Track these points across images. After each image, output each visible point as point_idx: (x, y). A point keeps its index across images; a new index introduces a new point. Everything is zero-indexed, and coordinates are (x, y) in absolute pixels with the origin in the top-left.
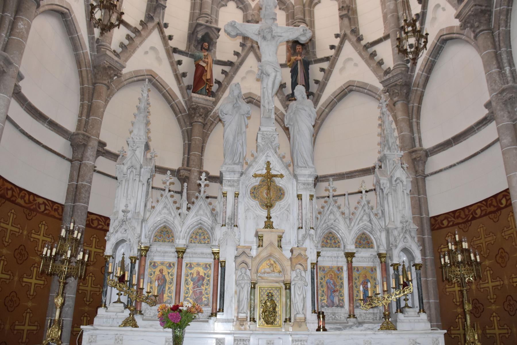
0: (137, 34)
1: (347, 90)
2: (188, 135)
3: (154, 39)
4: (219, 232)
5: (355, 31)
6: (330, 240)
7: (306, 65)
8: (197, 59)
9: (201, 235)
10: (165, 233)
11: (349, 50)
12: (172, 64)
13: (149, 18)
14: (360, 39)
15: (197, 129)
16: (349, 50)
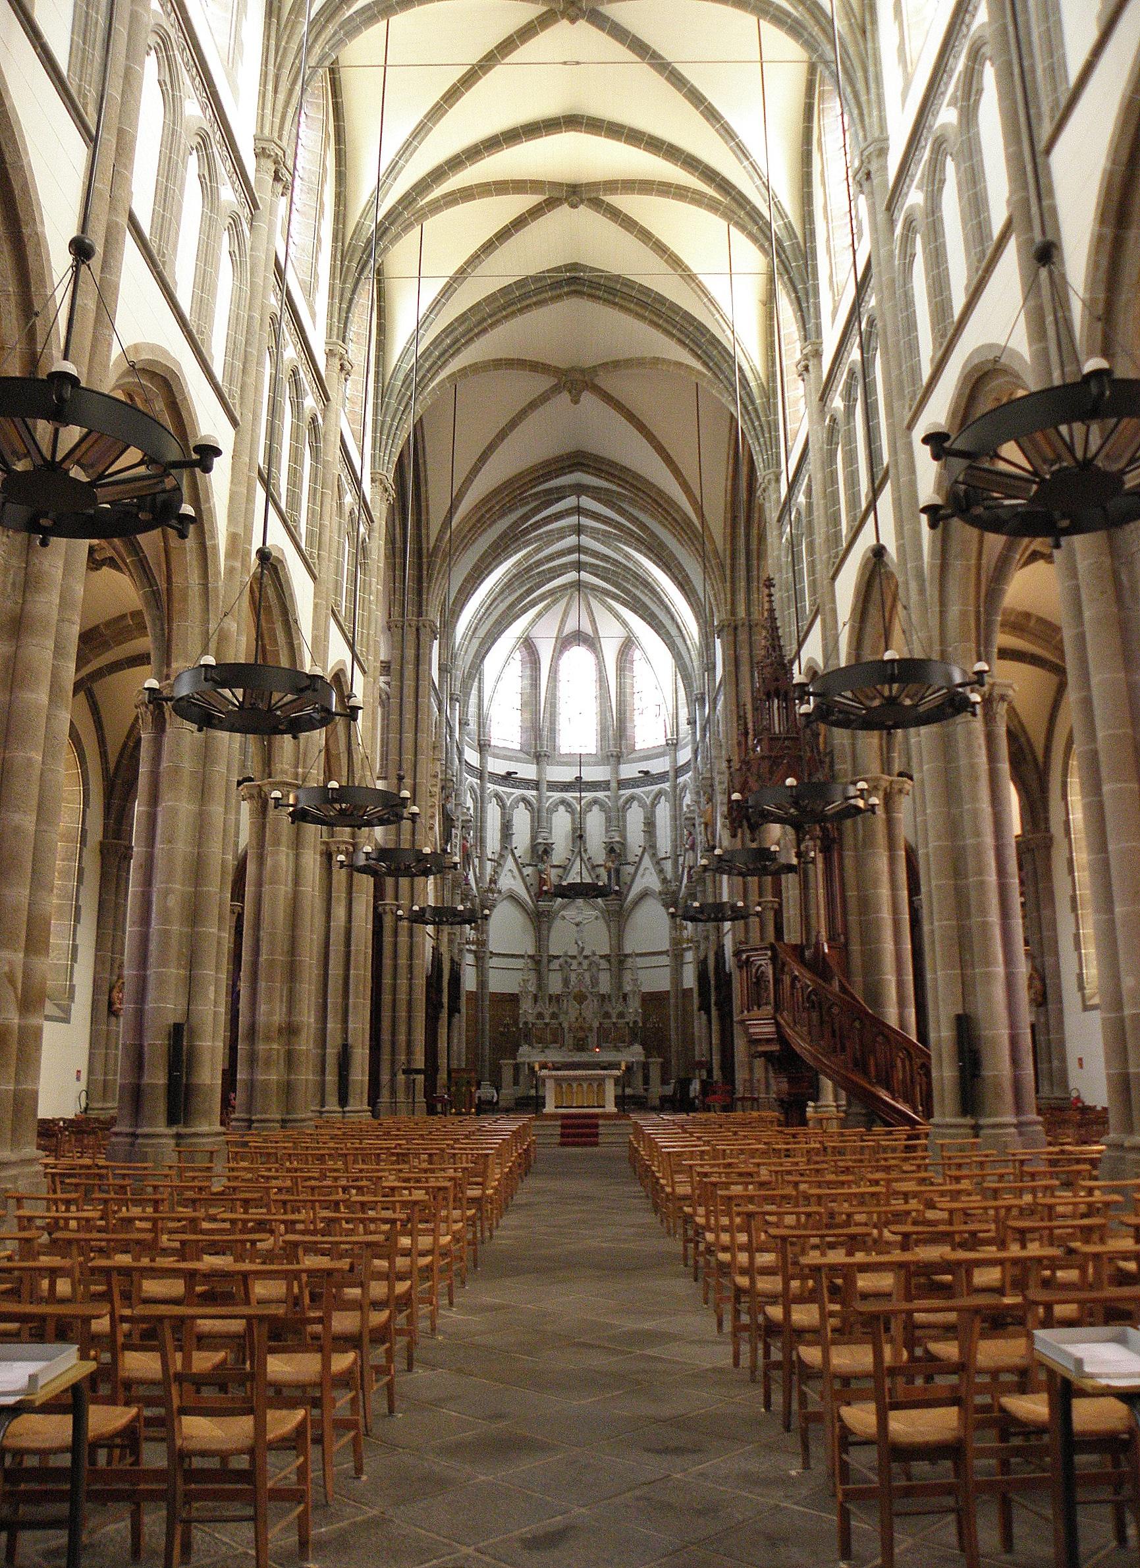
0: (499, 863)
1: (645, 895)
2: (538, 930)
3: (510, 863)
4: (562, 1018)
5: (653, 846)
6: (607, 1015)
7: (618, 871)
8: (540, 872)
9: (554, 1016)
10: (540, 1016)
11: (647, 861)
12: (523, 879)
13: (504, 848)
14: (654, 855)
15: (545, 926)
16: (647, 858)
